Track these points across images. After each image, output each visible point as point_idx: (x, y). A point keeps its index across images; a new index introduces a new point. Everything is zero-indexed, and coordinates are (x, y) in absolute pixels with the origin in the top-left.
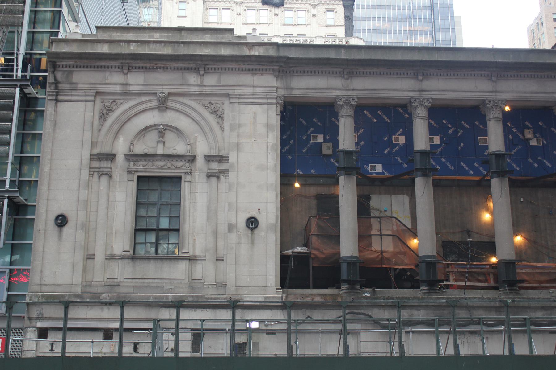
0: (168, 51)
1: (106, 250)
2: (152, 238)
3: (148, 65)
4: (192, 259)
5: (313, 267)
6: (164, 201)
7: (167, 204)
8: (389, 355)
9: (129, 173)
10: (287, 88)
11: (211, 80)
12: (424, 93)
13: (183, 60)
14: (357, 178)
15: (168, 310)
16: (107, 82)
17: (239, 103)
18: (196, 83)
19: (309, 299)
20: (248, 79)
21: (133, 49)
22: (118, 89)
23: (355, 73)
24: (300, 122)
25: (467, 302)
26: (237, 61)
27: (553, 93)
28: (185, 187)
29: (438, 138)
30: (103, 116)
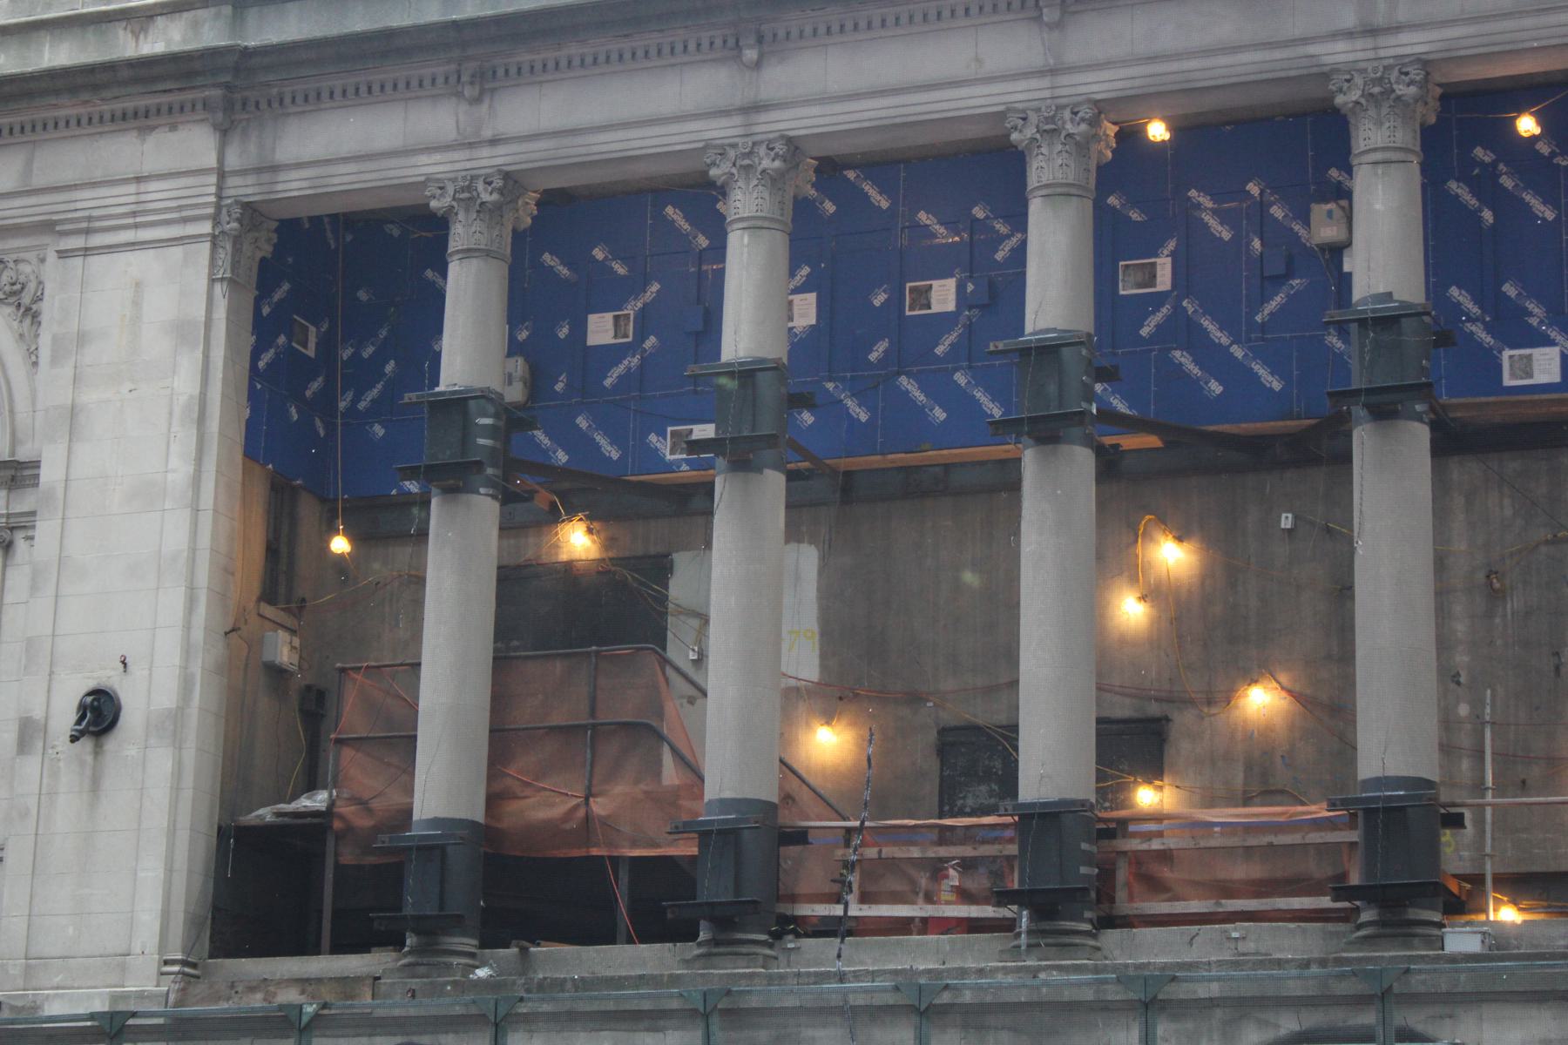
5: (337, 865)
10: (258, 170)
12: (763, 117)
17: (87, 252)
19: (256, 1001)
23: (501, 72)
26: (73, 90)
27: (1305, 41)
29: (951, 283)
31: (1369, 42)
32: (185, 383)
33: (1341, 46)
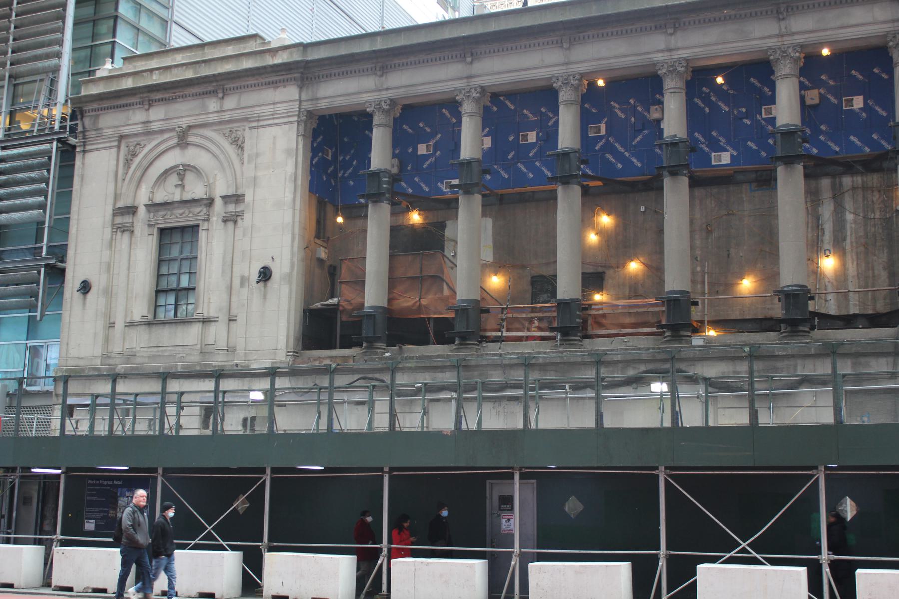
0: (189, 74)
1: (126, 316)
2: (171, 299)
3: (167, 96)
4: (206, 321)
5: (341, 322)
6: (185, 255)
7: (187, 258)
8: (419, 430)
9: (150, 226)
10: (312, 100)
11: (230, 102)
12: (473, 80)
13: (198, 84)
14: (804, 167)
15: (178, 381)
16: (130, 122)
17: (258, 127)
18: (215, 110)
19: (317, 363)
20: (270, 95)
21: (156, 79)
22: (139, 129)
24: (333, 141)
25: (502, 360)
26: (253, 75)
28: (202, 235)
29: (535, 133)
30: (128, 163)
31: (669, 54)
32: (290, 168)
33: (660, 55)
